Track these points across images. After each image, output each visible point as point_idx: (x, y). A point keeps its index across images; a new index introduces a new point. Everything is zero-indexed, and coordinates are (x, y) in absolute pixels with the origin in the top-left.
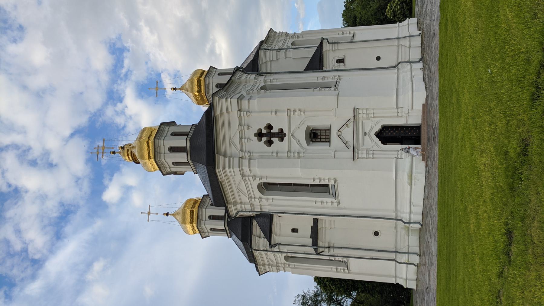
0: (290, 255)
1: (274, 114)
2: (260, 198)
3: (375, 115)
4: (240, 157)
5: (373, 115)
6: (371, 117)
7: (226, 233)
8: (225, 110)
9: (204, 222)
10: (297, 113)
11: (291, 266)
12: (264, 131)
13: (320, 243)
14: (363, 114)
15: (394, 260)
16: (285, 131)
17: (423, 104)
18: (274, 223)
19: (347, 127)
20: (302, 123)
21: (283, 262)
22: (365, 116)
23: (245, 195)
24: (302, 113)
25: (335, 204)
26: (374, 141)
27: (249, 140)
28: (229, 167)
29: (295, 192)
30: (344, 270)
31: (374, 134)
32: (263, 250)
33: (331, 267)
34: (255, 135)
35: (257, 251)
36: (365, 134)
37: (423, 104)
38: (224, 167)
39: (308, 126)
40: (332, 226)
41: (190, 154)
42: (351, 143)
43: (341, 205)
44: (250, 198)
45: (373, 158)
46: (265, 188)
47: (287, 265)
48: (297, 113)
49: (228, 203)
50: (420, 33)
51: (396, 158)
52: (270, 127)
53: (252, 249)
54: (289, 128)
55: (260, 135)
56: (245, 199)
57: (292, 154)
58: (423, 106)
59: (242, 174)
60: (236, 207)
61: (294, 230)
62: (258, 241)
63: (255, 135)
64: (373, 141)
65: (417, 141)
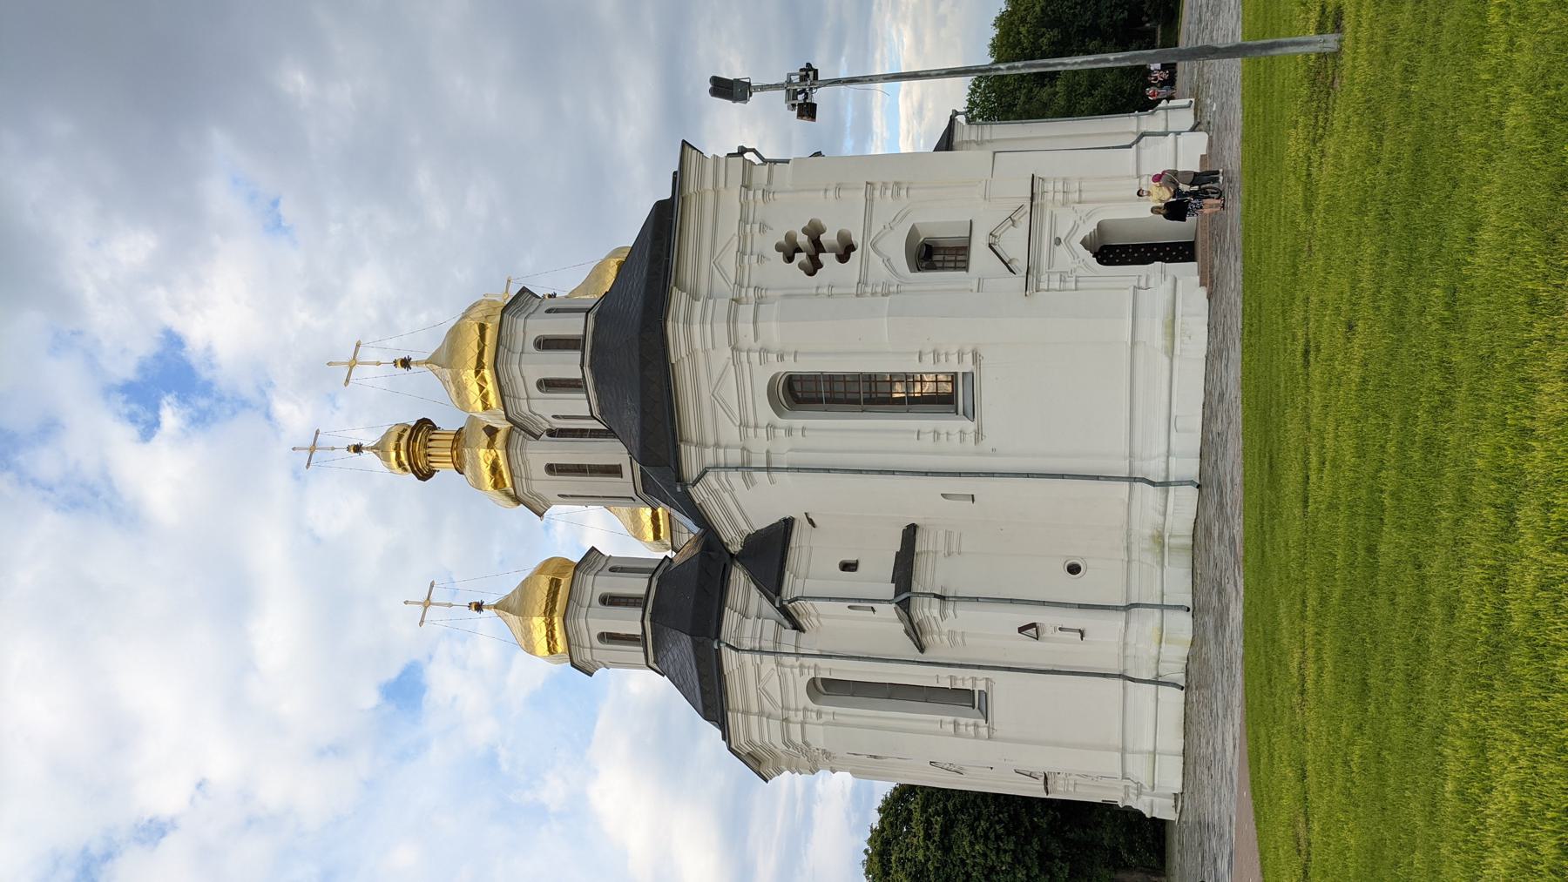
2: (771, 426)
3: (1084, 196)
4: (735, 297)
5: (1080, 195)
6: (1075, 202)
7: (641, 649)
8: (709, 184)
9: (584, 610)
10: (889, 192)
11: (825, 718)
12: (803, 240)
13: (916, 587)
14: (1055, 192)
15: (1119, 676)
16: (857, 239)
17: (1202, 156)
18: (793, 543)
19: (1013, 225)
20: (900, 216)
21: (801, 707)
22: (1059, 196)
23: (731, 419)
25: (970, 438)
26: (1078, 257)
27: (761, 258)
28: (703, 322)
29: (864, 413)
30: (976, 726)
31: (1083, 243)
32: (751, 651)
33: (939, 717)
35: (733, 652)
36: (1058, 241)
37: (1202, 156)
38: (688, 321)
39: (913, 226)
40: (954, 549)
41: (592, 351)
42: (1020, 265)
43: (987, 444)
44: (743, 425)
45: (1076, 289)
46: (785, 404)
47: (814, 715)
48: (889, 192)
49: (681, 441)
50: (1191, 102)
51: (1135, 287)
52: (814, 232)
53: (720, 642)
54: (867, 228)
55: (789, 251)
56: (731, 433)
57: (869, 290)
58: (1201, 160)
59: (733, 343)
60: (701, 457)
61: (848, 567)
62: (740, 625)
63: (779, 248)
64: (1076, 257)
65: (1191, 258)
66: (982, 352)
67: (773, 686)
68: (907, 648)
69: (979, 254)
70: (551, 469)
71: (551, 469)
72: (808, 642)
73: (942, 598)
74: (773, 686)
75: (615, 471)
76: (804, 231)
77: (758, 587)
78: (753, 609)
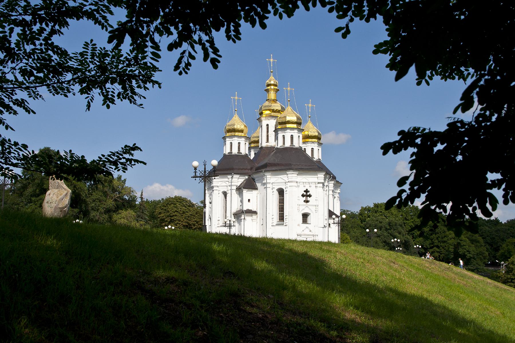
0: (228, 196)
1: (316, 199)
8: (319, 176)
12: (308, 194)
24: (316, 212)
25: (273, 224)
30: (219, 224)
32: (231, 181)
34: (307, 189)
52: (310, 196)
55: (307, 191)
61: (249, 200)
62: (236, 178)
63: (307, 189)
66: (287, 227)
67: (224, 184)
68: (234, 210)
69: (305, 225)
70: (267, 125)
71: (267, 125)
72: (234, 192)
73: (244, 219)
74: (224, 184)
75: (268, 141)
76: (310, 194)
77: (244, 181)
78: (239, 180)
